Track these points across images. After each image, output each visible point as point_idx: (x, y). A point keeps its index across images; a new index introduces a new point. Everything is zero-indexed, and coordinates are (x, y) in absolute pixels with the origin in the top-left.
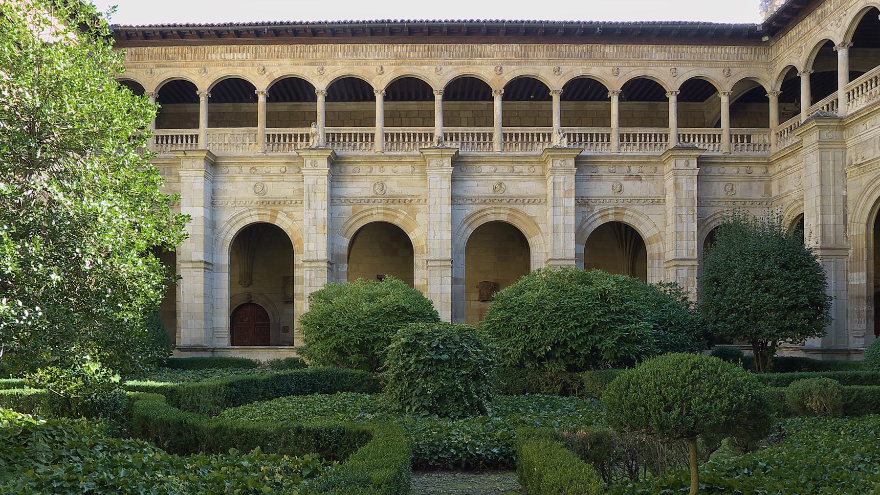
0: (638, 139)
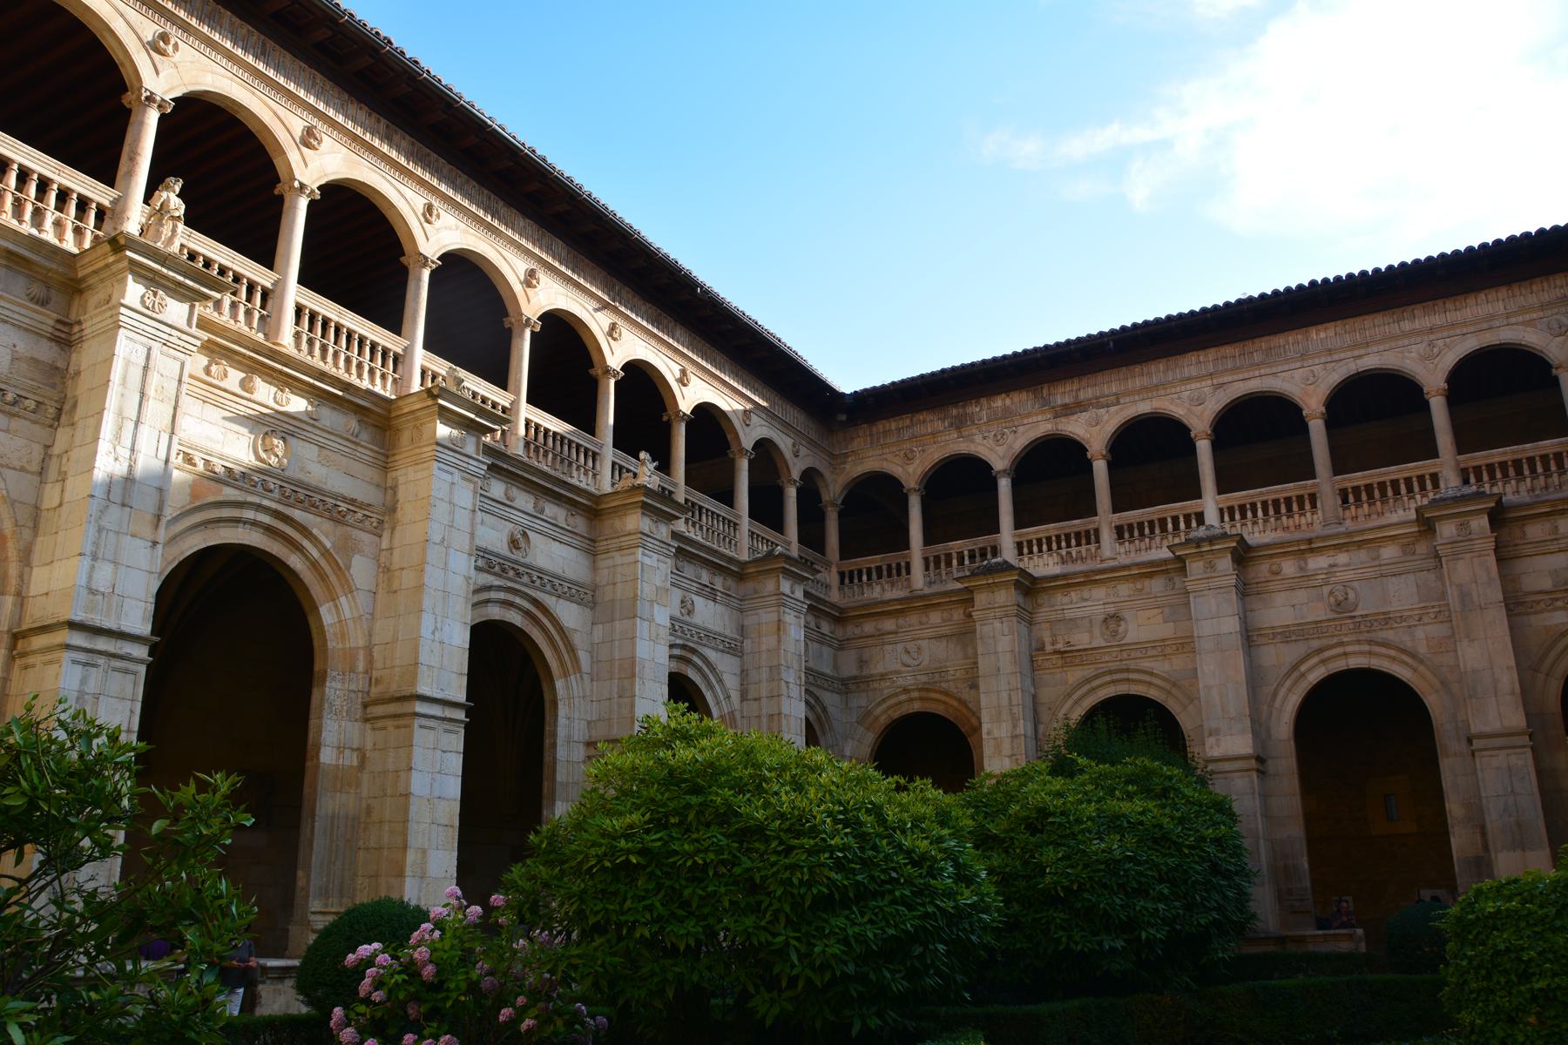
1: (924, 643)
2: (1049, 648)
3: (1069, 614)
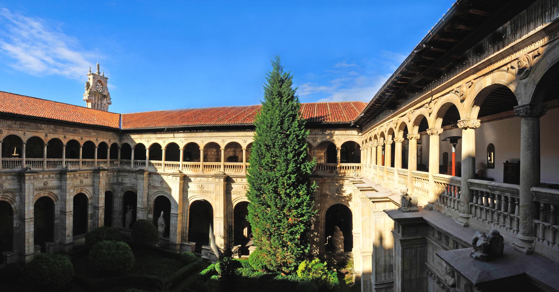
1: (132, 179)
2: (151, 185)
3: (155, 179)
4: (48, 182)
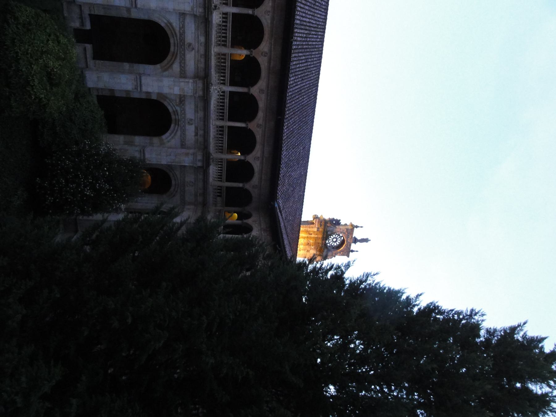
0: (220, 136)
4: (194, 51)
